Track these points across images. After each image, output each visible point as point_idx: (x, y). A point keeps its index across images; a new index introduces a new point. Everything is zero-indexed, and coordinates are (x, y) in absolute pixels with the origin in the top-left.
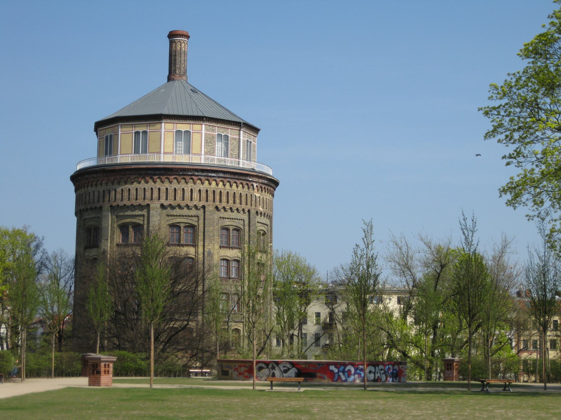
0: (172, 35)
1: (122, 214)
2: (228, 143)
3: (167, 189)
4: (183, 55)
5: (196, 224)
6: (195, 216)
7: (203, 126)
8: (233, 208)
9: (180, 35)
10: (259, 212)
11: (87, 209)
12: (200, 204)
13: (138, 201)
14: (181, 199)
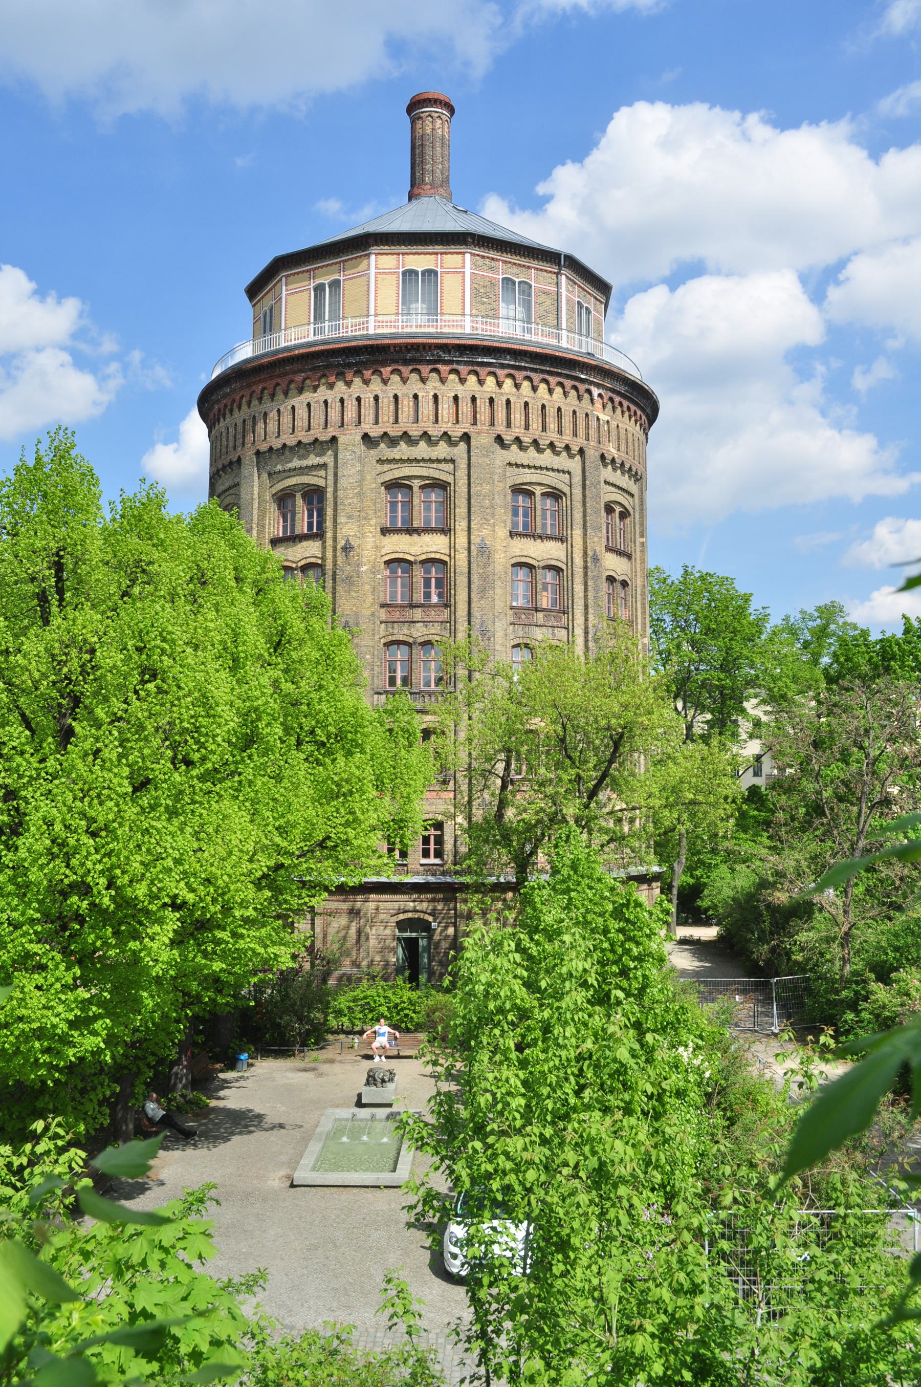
1: (279, 467)
2: (529, 302)
3: (376, 398)
4: (438, 144)
5: (450, 479)
6: (445, 461)
7: (468, 256)
8: (541, 442)
9: (429, 100)
10: (609, 458)
11: (218, 471)
12: (457, 432)
13: (312, 432)
14: (411, 419)
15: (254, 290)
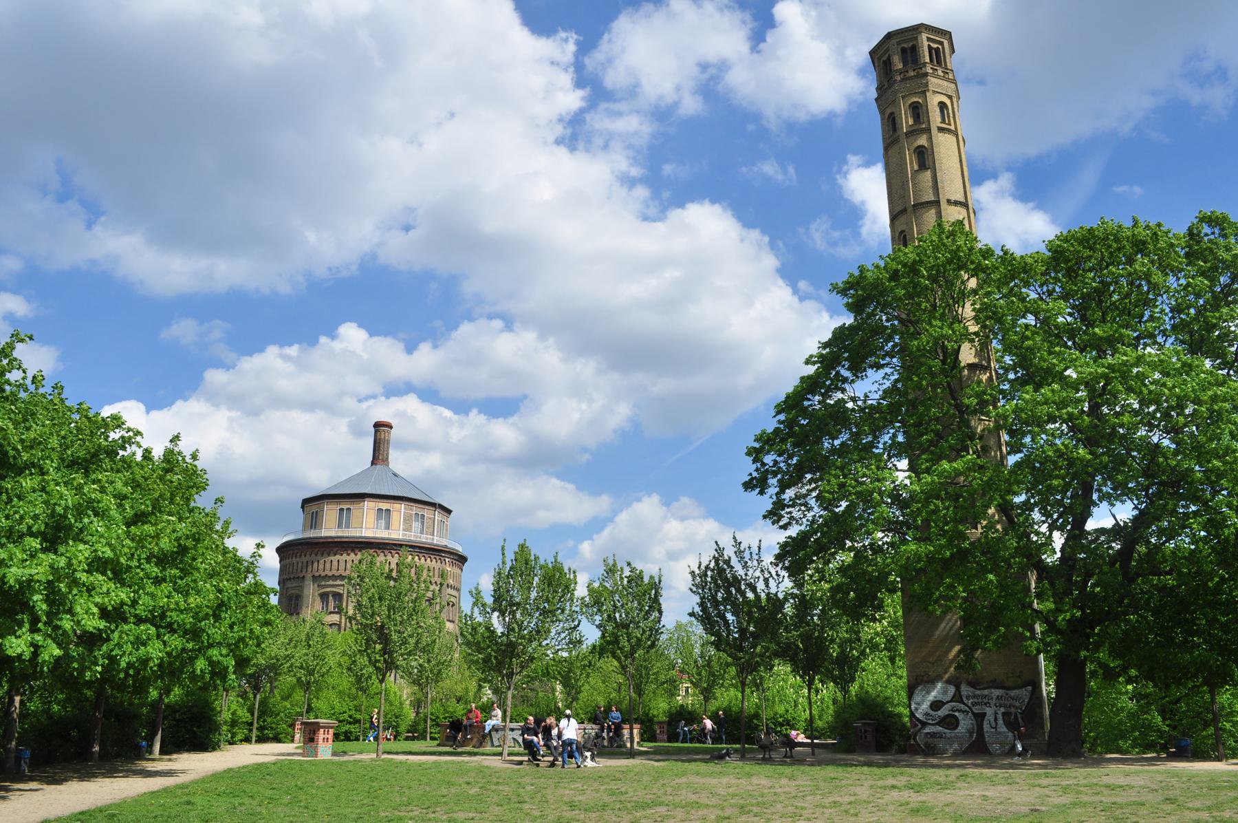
0: (378, 425)
15: (306, 502)
